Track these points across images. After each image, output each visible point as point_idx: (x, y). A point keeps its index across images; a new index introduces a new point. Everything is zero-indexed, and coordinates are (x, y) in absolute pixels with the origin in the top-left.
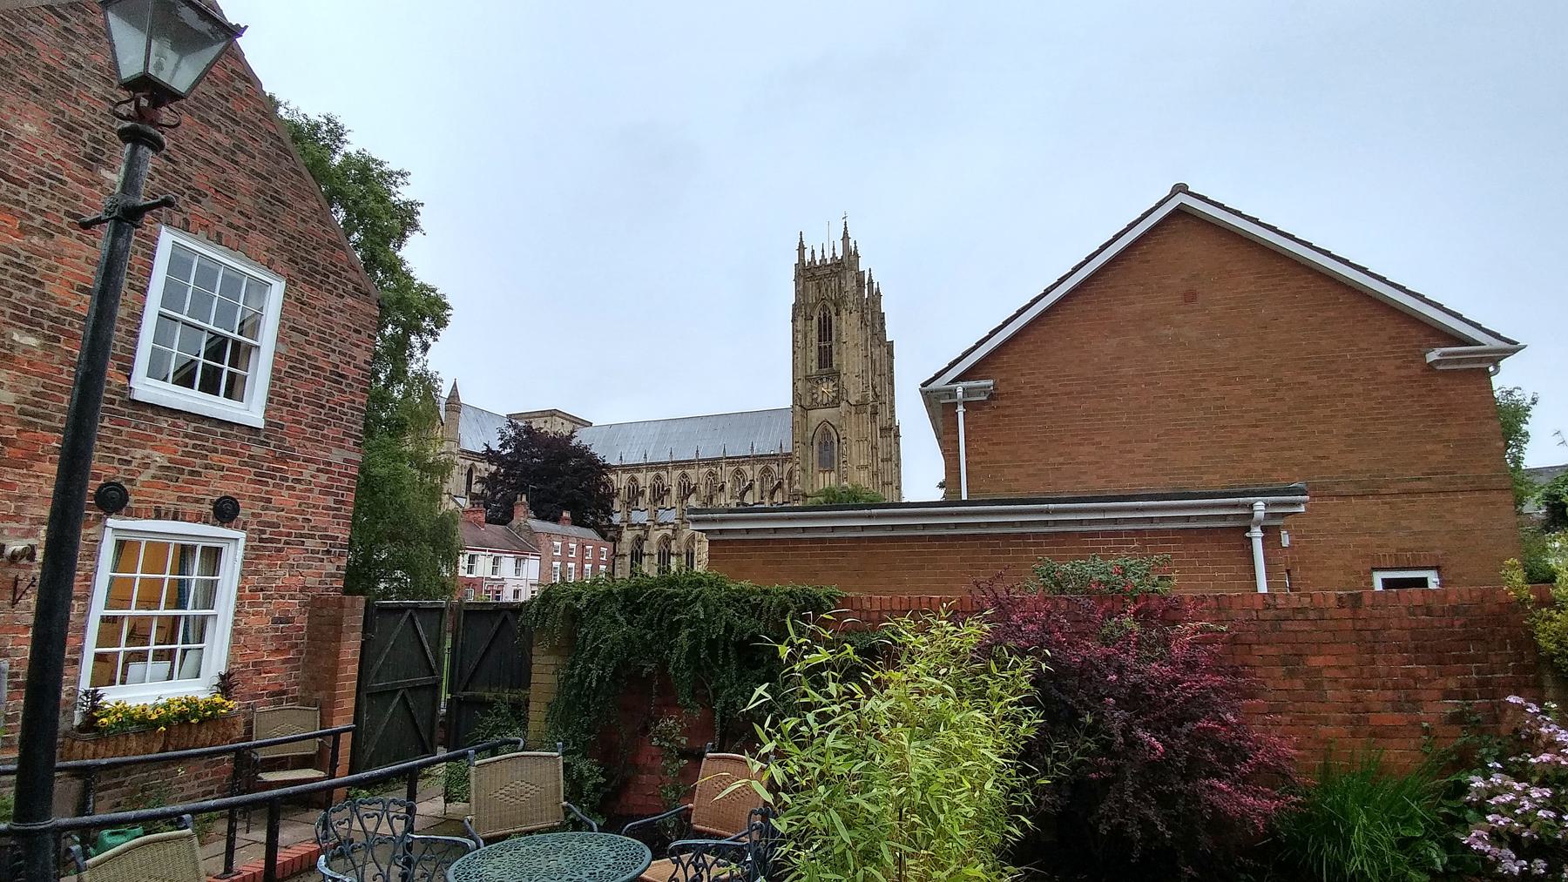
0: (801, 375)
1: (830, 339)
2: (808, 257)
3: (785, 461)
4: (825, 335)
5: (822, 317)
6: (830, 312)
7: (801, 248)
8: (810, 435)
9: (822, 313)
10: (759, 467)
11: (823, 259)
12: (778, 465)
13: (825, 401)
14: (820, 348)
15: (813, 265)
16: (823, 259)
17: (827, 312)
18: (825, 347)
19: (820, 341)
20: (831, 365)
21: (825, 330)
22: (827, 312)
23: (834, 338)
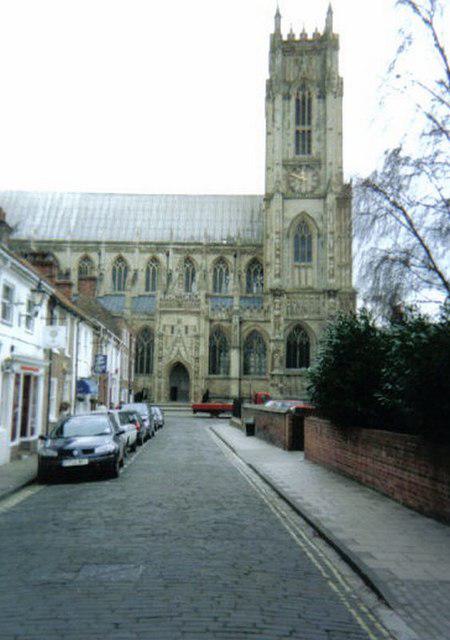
0: (278, 158)
1: (309, 123)
3: (244, 253)
5: (300, 98)
6: (309, 94)
8: (287, 225)
9: (301, 93)
10: (212, 258)
11: (304, 35)
12: (235, 256)
13: (304, 190)
14: (297, 132)
19: (297, 123)
20: (309, 152)
22: (307, 93)
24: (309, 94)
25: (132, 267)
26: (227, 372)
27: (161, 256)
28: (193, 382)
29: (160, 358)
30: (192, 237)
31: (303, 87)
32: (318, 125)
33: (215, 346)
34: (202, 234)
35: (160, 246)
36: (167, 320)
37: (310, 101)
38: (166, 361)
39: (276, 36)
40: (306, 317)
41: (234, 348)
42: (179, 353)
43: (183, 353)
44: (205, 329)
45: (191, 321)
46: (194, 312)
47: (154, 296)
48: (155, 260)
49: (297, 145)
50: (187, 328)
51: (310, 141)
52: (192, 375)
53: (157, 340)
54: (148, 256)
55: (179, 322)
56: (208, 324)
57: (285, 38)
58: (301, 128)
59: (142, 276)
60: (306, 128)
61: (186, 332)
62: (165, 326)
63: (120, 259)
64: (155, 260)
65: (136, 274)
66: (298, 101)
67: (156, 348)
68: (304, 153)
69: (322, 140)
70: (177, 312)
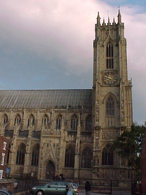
1: (112, 56)
2: (101, 23)
4: (110, 54)
7: (98, 18)
9: (108, 45)
11: (109, 23)
14: (107, 60)
15: (104, 25)
16: (109, 23)
17: (111, 45)
18: (110, 59)
19: (107, 56)
20: (113, 68)
21: (110, 51)
22: (111, 45)
23: (114, 55)
24: (112, 45)
26: (73, 166)
27: (49, 114)
31: (109, 42)
32: (116, 57)
33: (68, 154)
37: (112, 48)
38: (44, 160)
39: (97, 25)
40: (111, 140)
41: (76, 154)
42: (50, 156)
43: (52, 157)
44: (63, 145)
45: (57, 141)
46: (58, 137)
48: (46, 115)
49: (107, 65)
50: (54, 144)
51: (113, 63)
56: (65, 142)
57: (101, 25)
58: (109, 58)
60: (111, 58)
61: (54, 147)
62: (44, 143)
66: (107, 48)
68: (110, 68)
69: (118, 62)
70: (50, 137)
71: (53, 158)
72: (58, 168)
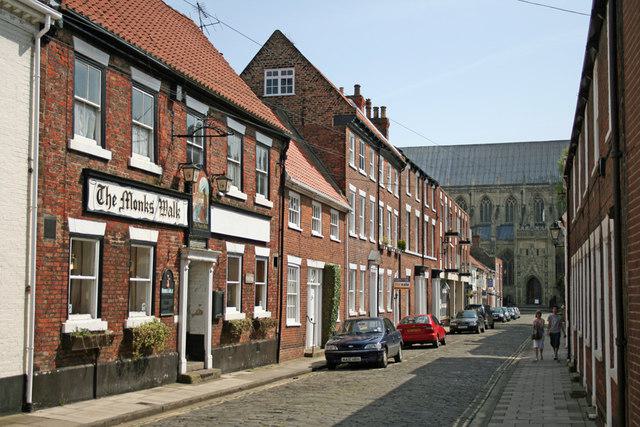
25: (495, 203)
27: (517, 195)
28: (544, 290)
29: (519, 273)
30: (541, 178)
34: (549, 174)
35: (515, 186)
36: (522, 245)
42: (532, 269)
45: (542, 245)
47: (512, 225)
48: (512, 197)
52: (543, 285)
53: (516, 260)
54: (506, 195)
55: (532, 246)
59: (503, 210)
62: (521, 250)
63: (486, 198)
64: (512, 197)
65: (498, 210)
67: (516, 266)
70: (530, 239)
71: (538, 273)
72: (547, 287)
